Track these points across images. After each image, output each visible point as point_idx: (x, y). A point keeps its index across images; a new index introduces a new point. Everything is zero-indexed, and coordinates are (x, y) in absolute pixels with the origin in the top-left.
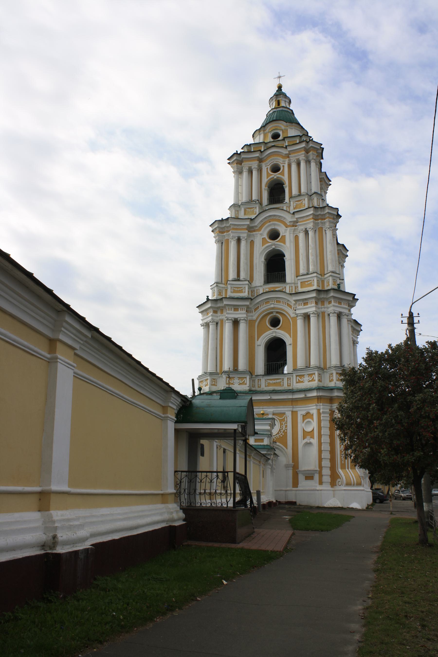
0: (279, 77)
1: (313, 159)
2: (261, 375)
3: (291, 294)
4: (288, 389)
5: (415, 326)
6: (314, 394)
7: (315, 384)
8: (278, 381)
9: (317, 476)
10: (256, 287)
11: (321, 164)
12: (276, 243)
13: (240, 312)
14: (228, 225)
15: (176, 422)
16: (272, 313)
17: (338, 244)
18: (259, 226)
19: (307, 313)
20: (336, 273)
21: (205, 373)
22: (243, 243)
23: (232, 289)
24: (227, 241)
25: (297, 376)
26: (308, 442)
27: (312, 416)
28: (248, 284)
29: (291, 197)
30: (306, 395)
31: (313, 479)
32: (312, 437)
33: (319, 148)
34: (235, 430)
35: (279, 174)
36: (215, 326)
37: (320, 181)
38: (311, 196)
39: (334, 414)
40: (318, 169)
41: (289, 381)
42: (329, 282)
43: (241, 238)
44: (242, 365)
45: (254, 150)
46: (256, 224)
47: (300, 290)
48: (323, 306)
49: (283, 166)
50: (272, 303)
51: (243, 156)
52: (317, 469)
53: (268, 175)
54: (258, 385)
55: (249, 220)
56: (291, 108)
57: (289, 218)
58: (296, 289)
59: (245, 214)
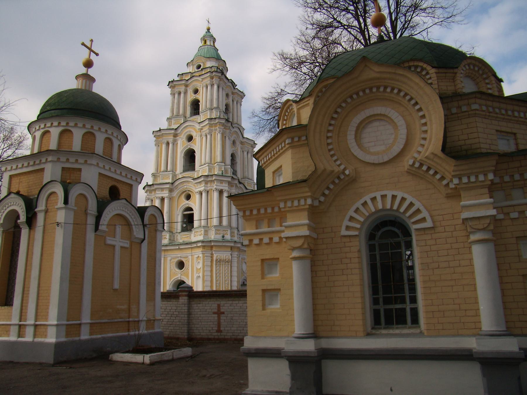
7: (201, 238)
13: (165, 192)
14: (161, 134)
19: (200, 191)
22: (171, 145)
25: (195, 232)
28: (172, 174)
30: (197, 245)
36: (151, 202)
45: (181, 79)
49: (200, 89)
53: (191, 96)
57: (198, 127)
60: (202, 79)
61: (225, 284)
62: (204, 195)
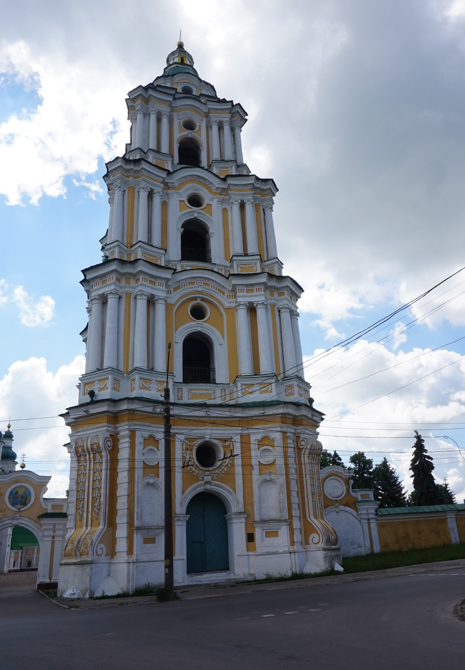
12: (200, 211)
13: (157, 286)
21: (98, 369)
27: (272, 443)
31: (277, 536)
50: (200, 284)
55: (166, 173)
60: (209, 109)
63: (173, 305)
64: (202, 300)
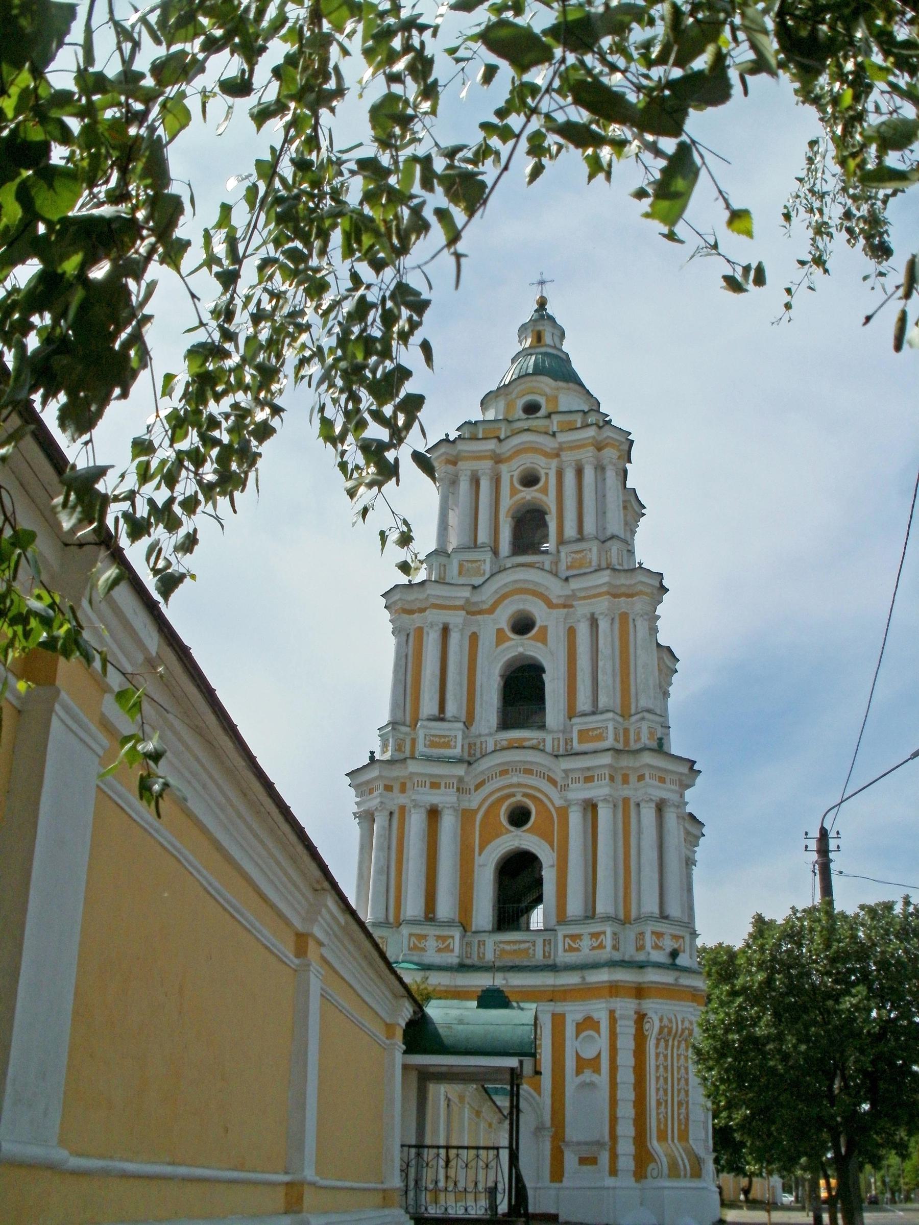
0: (542, 283)
1: (610, 462)
2: (485, 932)
3: (556, 756)
4: (546, 963)
5: (832, 856)
6: (603, 976)
8: (523, 946)
9: (604, 1158)
10: (480, 735)
11: (625, 472)
14: (425, 596)
15: (405, 1052)
16: (513, 795)
17: (658, 645)
18: (490, 602)
20: (656, 714)
22: (454, 639)
23: (428, 738)
24: (420, 631)
25: (565, 937)
26: (588, 1080)
28: (464, 732)
29: (561, 542)
30: (583, 978)
32: (597, 1070)
33: (624, 440)
34: (512, 1070)
35: (536, 491)
36: (388, 818)
37: (625, 508)
38: (604, 542)
39: (646, 1020)
40: (619, 483)
41: (547, 946)
42: (639, 733)
43: (451, 626)
44: (445, 908)
46: (484, 598)
47: (577, 746)
48: (625, 786)
49: (547, 474)
51: (462, 446)
52: (607, 1138)
53: (514, 492)
54: (479, 953)
55: (470, 588)
56: (565, 348)
57: (555, 589)
58: (566, 744)
59: (460, 573)
61: (679, 1114)
62: (604, 814)
63: (476, 811)
64: (525, 795)
